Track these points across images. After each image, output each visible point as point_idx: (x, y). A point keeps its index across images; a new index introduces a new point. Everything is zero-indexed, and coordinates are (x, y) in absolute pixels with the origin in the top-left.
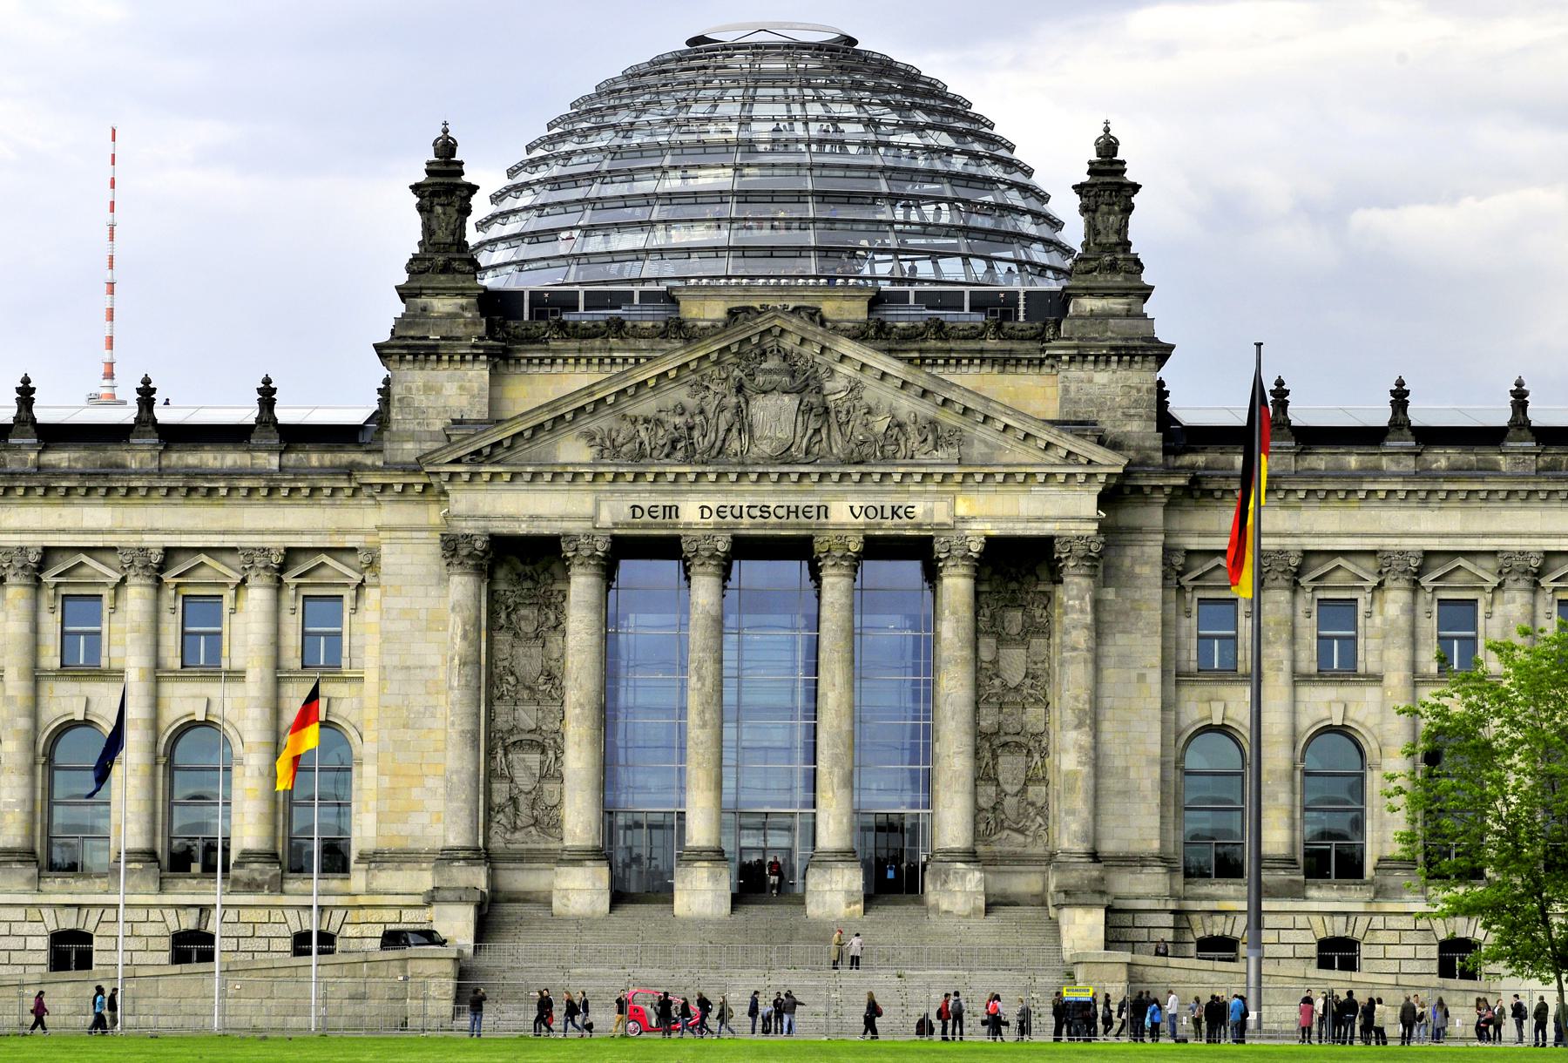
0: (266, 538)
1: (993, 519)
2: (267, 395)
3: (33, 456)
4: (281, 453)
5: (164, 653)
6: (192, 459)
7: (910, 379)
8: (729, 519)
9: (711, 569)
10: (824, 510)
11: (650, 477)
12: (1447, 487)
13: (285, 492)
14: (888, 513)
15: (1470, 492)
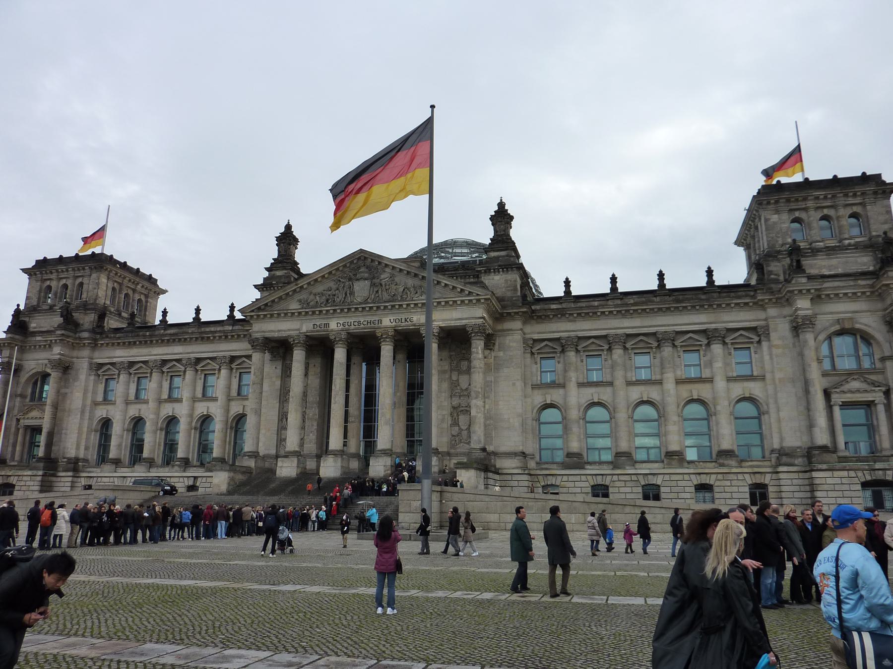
0: (226, 353)
1: (443, 320)
2: (232, 308)
3: (162, 331)
4: (233, 326)
5: (196, 393)
6: (208, 329)
7: (409, 270)
8: (347, 327)
9: (340, 345)
10: (380, 321)
11: (317, 313)
12: (632, 308)
13: (230, 337)
14: (403, 321)
15: (642, 310)
